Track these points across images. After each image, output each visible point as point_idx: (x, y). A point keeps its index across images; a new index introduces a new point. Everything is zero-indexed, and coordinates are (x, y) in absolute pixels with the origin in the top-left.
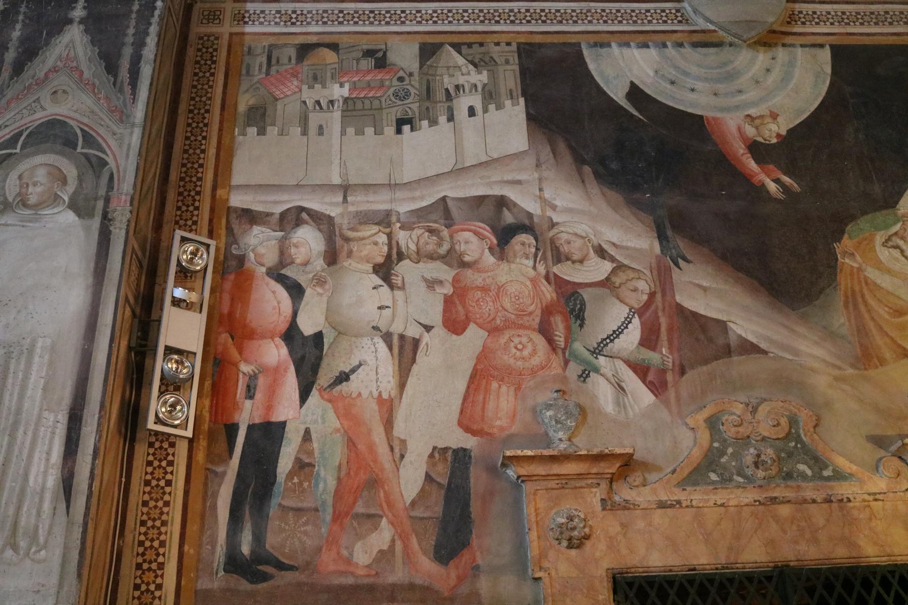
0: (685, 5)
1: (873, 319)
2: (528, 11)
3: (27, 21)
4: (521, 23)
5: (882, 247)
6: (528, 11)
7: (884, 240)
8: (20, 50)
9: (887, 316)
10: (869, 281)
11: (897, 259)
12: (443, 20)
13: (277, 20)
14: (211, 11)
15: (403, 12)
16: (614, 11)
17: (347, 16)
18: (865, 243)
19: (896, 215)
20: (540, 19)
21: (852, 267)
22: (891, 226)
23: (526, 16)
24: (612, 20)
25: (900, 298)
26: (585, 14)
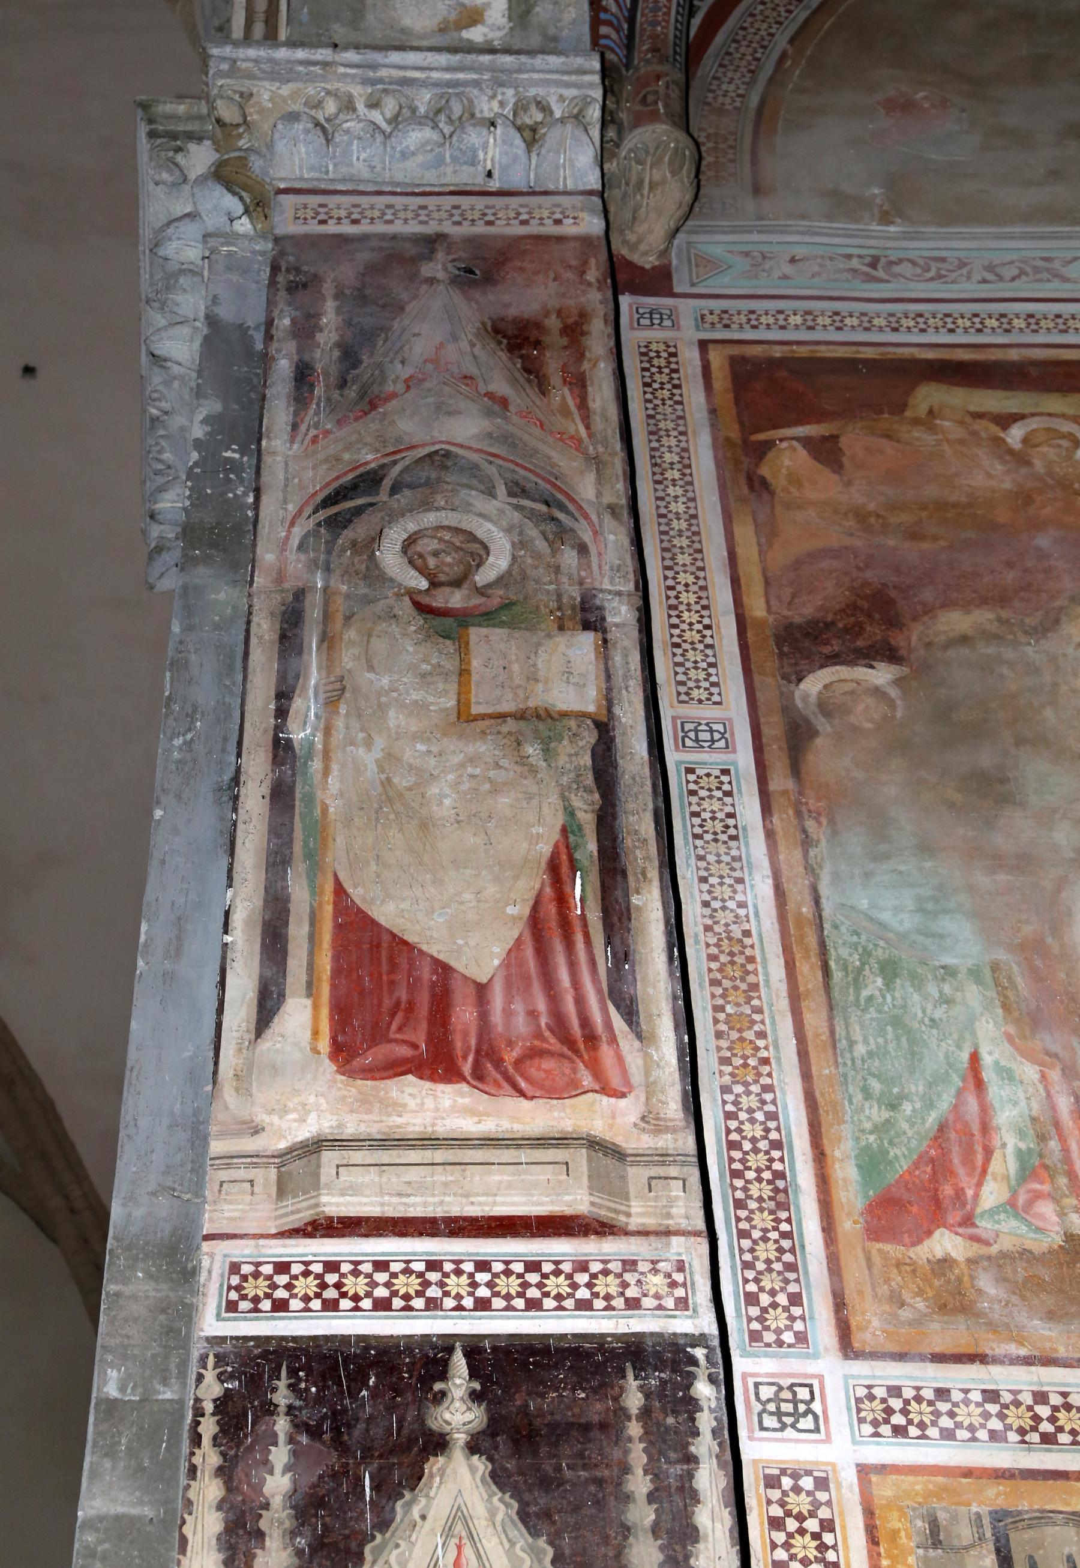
3: (304, 1439)
8: (301, 1542)
13: (995, 1424)
14: (781, 1388)
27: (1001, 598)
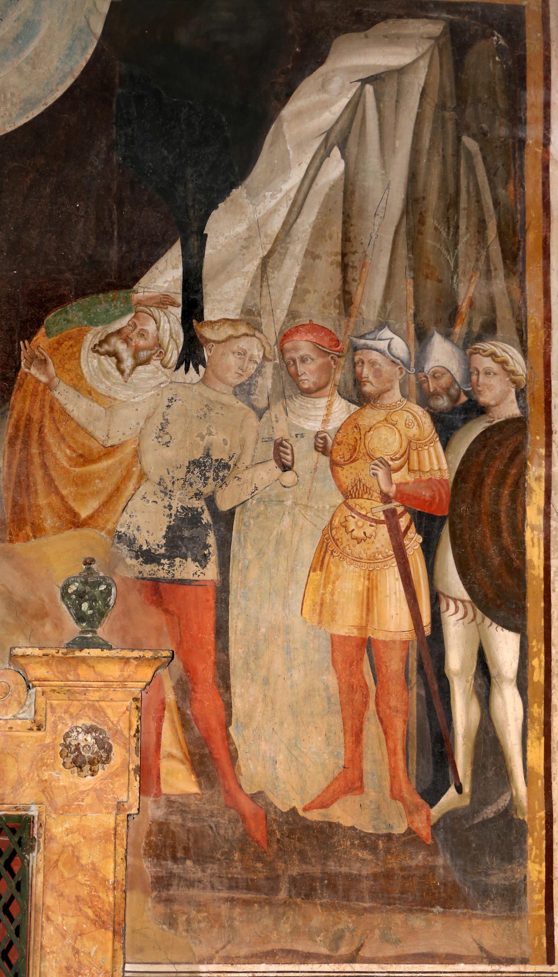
1: (44, 466)
5: (91, 354)
7: (97, 342)
9: (65, 464)
10: (57, 407)
11: (106, 374)
18: (68, 343)
19: (127, 300)
21: (38, 381)
22: (116, 318)
25: (93, 437)
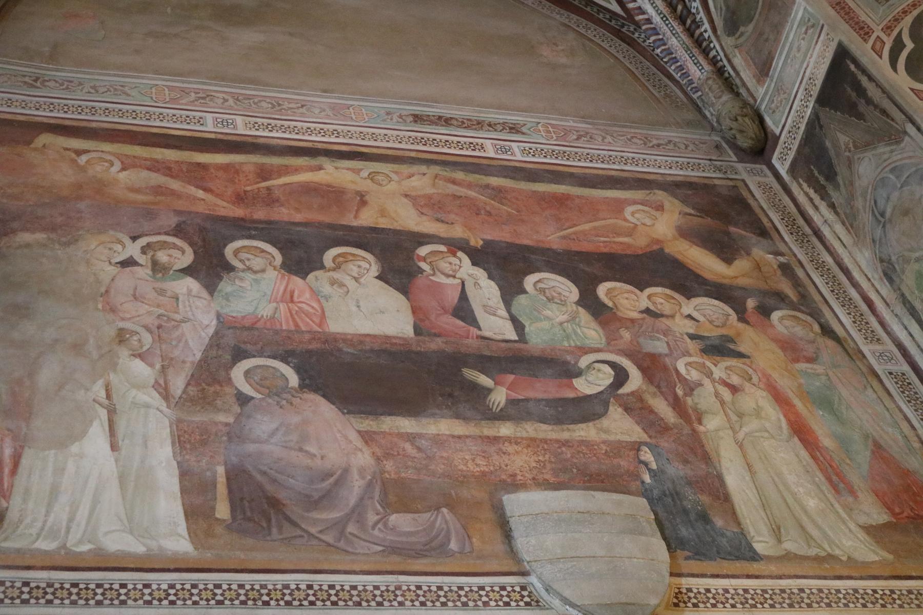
0: (533, 579)
2: (310, 587)
4: (301, 605)
6: (310, 587)
12: (184, 600)
15: (123, 586)
16: (434, 589)
17: (35, 591)
20: (329, 599)
23: (308, 595)
24: (433, 602)
26: (393, 592)
27: (53, 228)
